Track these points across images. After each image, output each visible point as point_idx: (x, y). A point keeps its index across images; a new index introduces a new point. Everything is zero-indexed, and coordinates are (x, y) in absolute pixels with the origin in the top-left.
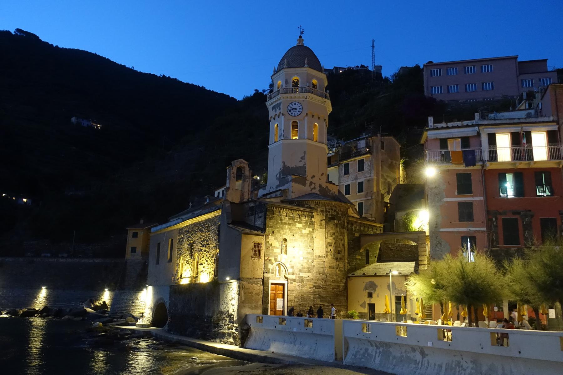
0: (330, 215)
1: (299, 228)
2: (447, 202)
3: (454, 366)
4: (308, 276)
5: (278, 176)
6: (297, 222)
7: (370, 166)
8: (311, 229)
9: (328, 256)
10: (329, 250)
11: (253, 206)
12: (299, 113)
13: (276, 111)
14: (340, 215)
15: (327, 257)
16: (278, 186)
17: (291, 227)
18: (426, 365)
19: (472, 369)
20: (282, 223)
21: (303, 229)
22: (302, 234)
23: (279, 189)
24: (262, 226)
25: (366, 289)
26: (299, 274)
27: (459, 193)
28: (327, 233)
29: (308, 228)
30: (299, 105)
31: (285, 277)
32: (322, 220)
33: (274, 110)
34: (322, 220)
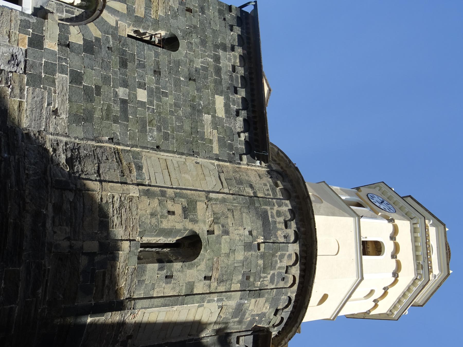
0: (272, 217)
1: (214, 103)
4: (55, 112)
6: (227, 99)
8: (216, 150)
9: (145, 200)
10: (170, 206)
14: (279, 265)
15: (148, 194)
17: (212, 76)
20: (217, 47)
21: (213, 116)
22: (200, 112)
26: (63, 71)
28: (224, 201)
29: (219, 139)
32: (251, 186)
34: (251, 186)
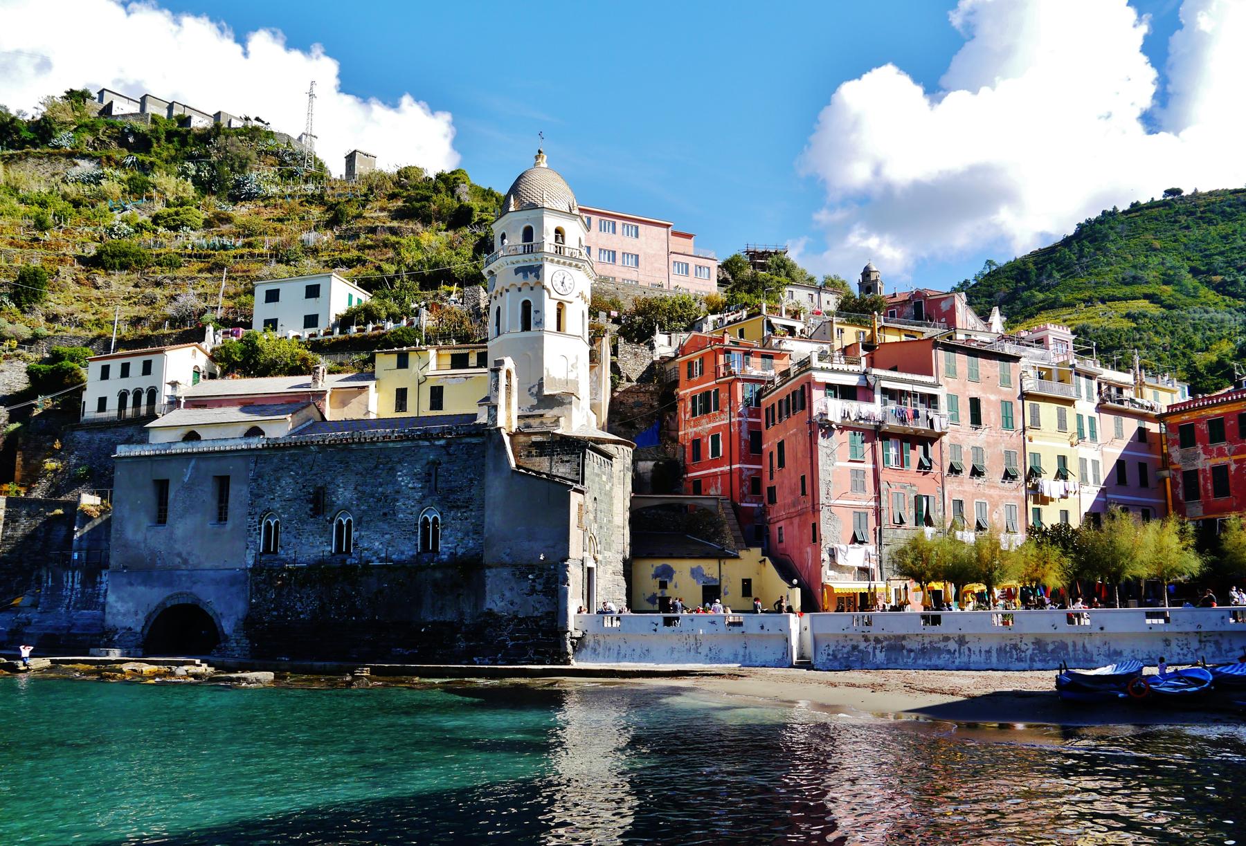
2: (839, 467)
3: (1008, 649)
5: (535, 390)
7: (596, 382)
11: (544, 442)
12: (569, 291)
13: (525, 276)
16: (533, 408)
18: (967, 652)
19: (1034, 649)
23: (537, 412)
24: (576, 478)
25: (655, 576)
27: (851, 456)
30: (569, 277)
31: (595, 559)
33: (521, 275)
